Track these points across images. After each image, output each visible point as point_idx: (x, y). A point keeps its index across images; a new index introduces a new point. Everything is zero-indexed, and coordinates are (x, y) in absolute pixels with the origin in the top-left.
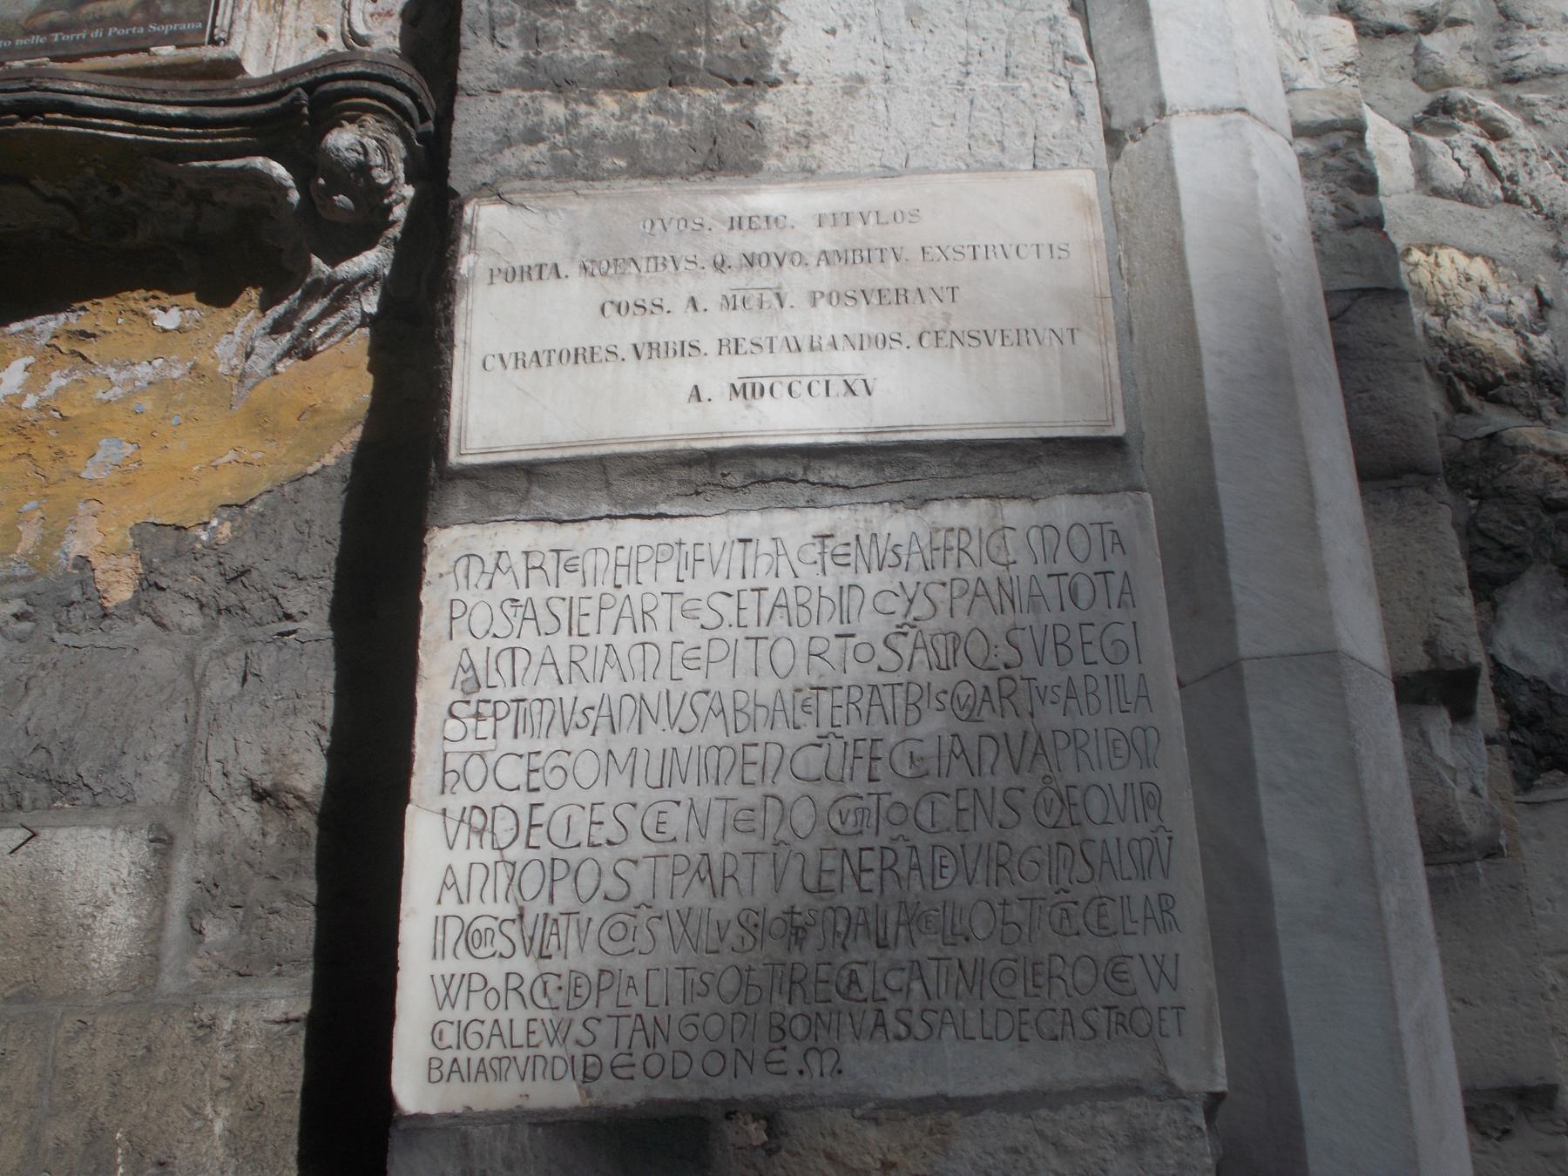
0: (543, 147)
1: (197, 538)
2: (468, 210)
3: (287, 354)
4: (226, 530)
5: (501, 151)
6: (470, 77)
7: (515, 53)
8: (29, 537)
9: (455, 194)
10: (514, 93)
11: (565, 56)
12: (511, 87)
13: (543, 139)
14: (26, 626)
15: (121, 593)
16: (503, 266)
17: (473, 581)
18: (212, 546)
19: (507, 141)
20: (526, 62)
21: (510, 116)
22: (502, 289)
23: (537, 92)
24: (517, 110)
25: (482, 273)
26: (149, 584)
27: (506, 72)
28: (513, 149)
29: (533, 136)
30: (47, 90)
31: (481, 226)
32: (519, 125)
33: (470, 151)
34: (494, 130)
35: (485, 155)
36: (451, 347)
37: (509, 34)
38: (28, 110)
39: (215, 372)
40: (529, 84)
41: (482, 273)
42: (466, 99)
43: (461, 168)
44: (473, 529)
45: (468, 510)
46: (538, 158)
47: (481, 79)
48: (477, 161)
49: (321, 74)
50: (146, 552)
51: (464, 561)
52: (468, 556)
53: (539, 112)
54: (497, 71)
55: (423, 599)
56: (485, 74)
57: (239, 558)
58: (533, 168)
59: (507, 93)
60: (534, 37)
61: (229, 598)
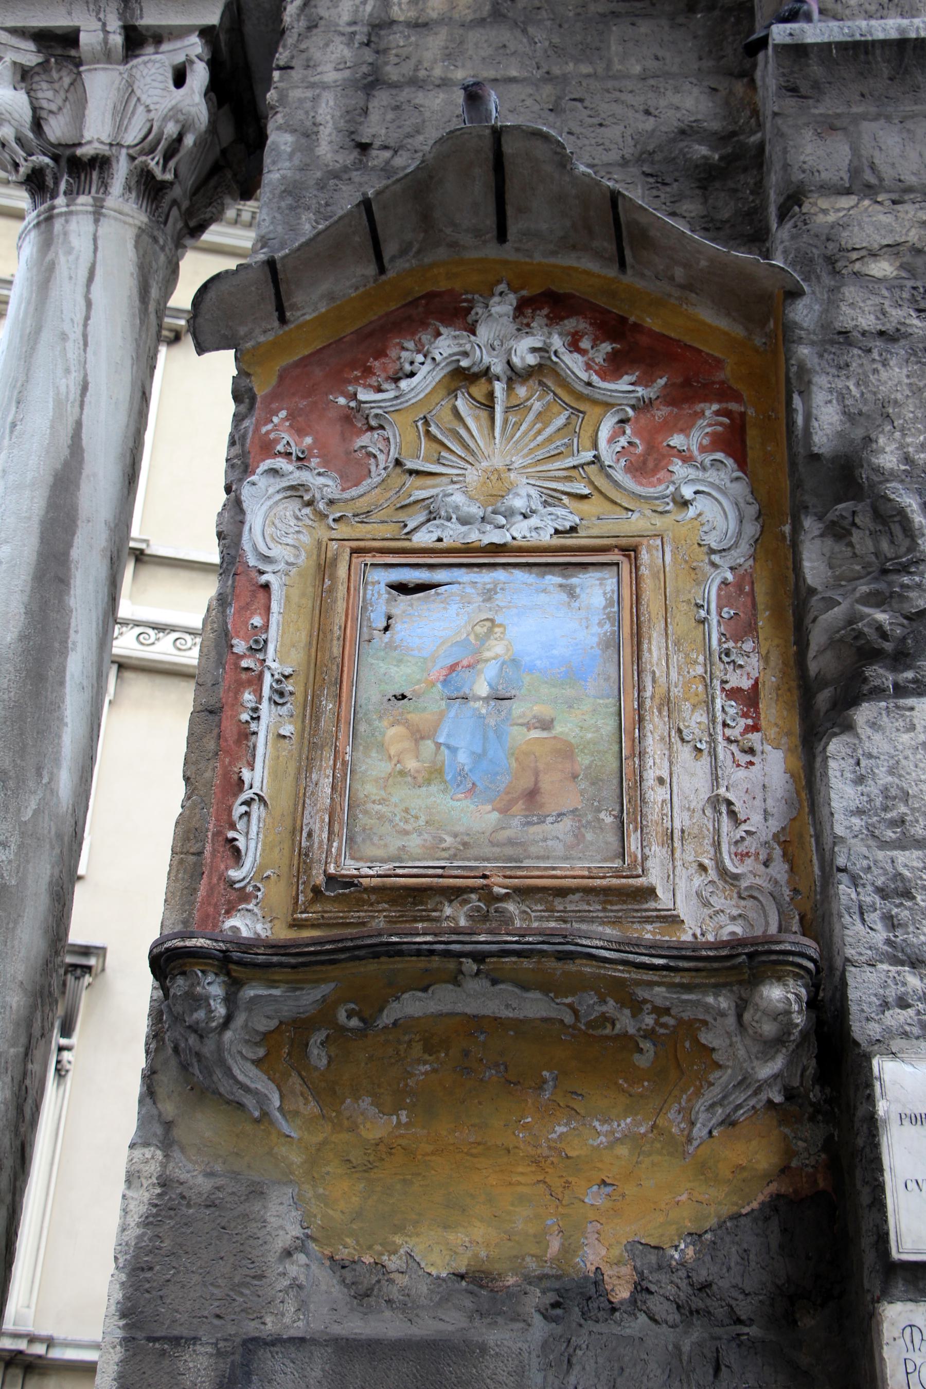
0: (911, 1012)
1: (672, 1257)
2: (875, 1062)
3: (722, 1123)
4: (690, 1251)
5: (883, 1012)
6: (853, 952)
7: (881, 935)
8: (555, 1245)
9: (857, 1044)
10: (885, 967)
11: (915, 940)
12: (881, 962)
13: (909, 1006)
14: (559, 1311)
15: (623, 1293)
16: (908, 1113)
17: (917, 1347)
18: (682, 1264)
19: (885, 1005)
20: (888, 942)
21: (885, 986)
22: (910, 1130)
23: (900, 968)
24: (889, 981)
25: (894, 1118)
26: (641, 1289)
27: (877, 949)
28: (891, 1012)
29: (903, 1003)
30: (577, 944)
31: (886, 1077)
32: (892, 993)
33: (863, 1011)
34: (876, 995)
35: (873, 1015)
36: (881, 1170)
37: (874, 918)
38: (563, 956)
39: (670, 1132)
40: (895, 961)
41: (894, 1118)
42: (853, 969)
43: (858, 1024)
44: (910, 1306)
45: (905, 1291)
46: (909, 1021)
47: (861, 954)
48: (868, 1019)
49: (760, 948)
50: (638, 1264)
51: (908, 1329)
52: (910, 1326)
53: (904, 984)
54: (870, 948)
55: (885, 1355)
56: (864, 951)
57: (702, 1276)
58: (907, 1028)
59: (880, 966)
60: (891, 922)
61: (697, 1303)
